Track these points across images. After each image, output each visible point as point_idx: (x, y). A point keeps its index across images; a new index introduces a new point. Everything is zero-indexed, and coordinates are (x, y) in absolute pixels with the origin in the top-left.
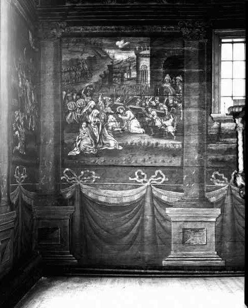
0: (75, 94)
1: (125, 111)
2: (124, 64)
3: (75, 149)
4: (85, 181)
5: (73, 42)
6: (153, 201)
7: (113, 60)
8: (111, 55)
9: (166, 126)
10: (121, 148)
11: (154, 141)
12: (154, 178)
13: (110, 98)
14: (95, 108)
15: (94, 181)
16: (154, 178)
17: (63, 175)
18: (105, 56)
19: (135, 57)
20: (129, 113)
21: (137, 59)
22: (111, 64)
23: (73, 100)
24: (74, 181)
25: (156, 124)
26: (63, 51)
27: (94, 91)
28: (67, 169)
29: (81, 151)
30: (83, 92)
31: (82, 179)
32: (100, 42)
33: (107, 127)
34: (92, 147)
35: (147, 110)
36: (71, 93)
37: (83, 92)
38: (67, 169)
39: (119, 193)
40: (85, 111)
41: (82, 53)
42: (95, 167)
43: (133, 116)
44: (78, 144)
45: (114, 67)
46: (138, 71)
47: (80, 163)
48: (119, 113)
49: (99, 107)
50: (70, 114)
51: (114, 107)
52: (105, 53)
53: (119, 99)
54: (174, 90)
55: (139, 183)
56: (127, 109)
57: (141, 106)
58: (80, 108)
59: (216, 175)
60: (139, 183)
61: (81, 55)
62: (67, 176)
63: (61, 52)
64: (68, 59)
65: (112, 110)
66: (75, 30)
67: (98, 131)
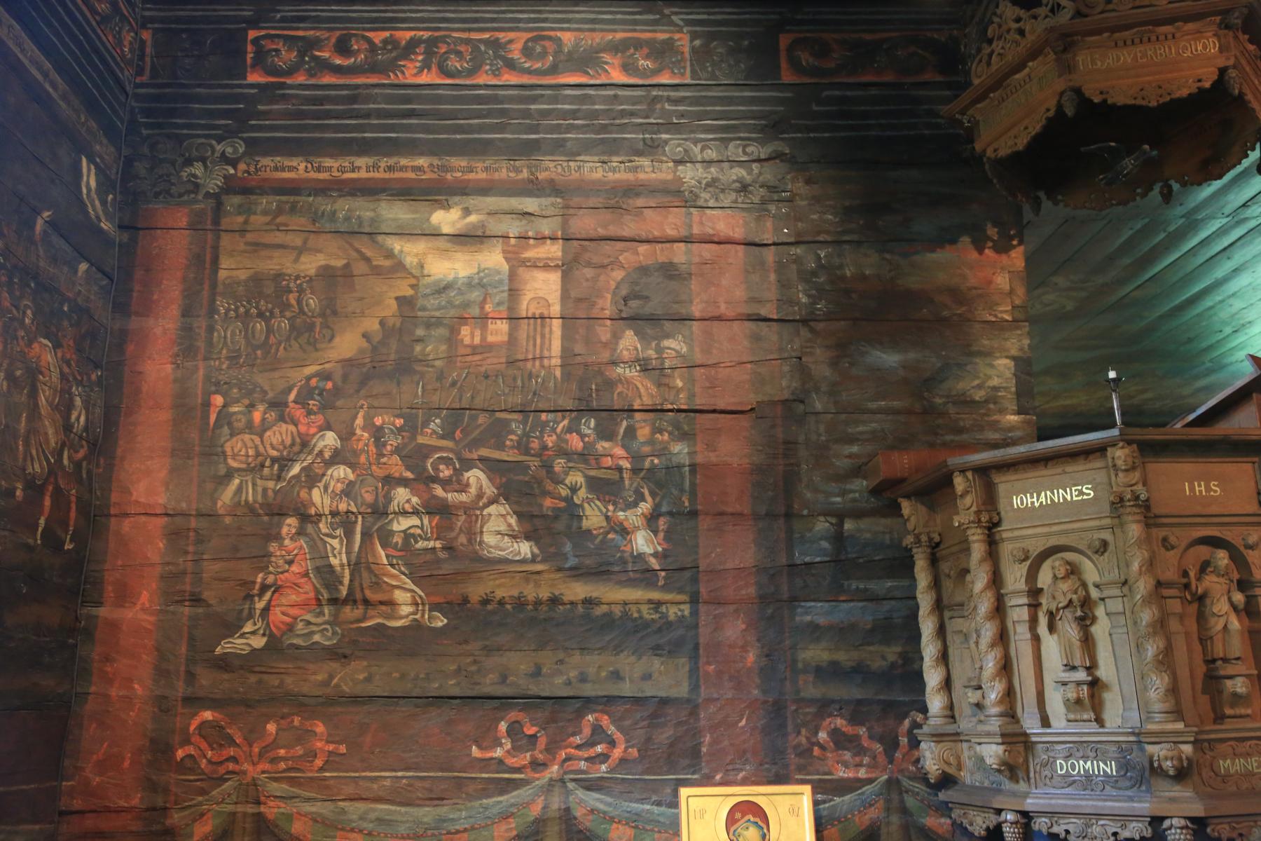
0: (261, 408)
1: (458, 473)
2: (461, 292)
3: (248, 628)
4: (283, 765)
5: (265, 213)
7: (416, 276)
8: (410, 261)
9: (624, 532)
10: (440, 622)
11: (578, 590)
12: (578, 747)
13: (399, 422)
14: (337, 458)
15: (319, 762)
16: (578, 747)
17: (187, 741)
18: (387, 263)
19: (506, 267)
20: (476, 477)
21: (512, 275)
22: (410, 292)
23: (250, 427)
24: (231, 766)
25: (586, 524)
26: (226, 241)
27: (337, 392)
28: (208, 715)
29: (271, 636)
30: (292, 397)
31: (271, 755)
32: (369, 214)
33: (386, 537)
34: (319, 620)
35: (548, 467)
36: (247, 402)
37: (292, 397)
38: (208, 715)
39: (427, 814)
40: (296, 470)
41: (300, 251)
42: (331, 703)
43: (490, 490)
44: (260, 605)
45: (420, 302)
46: (513, 319)
47: (255, 690)
48: (435, 479)
49: (356, 453)
50: (237, 481)
51: (415, 456)
52: (389, 254)
53: (435, 424)
54: (654, 390)
55: (518, 770)
56: (467, 465)
57: (527, 453)
58: (274, 460)
59: (835, 733)
60: (518, 770)
61: (296, 260)
62: (204, 745)
63: (216, 248)
64: (243, 275)
65: (408, 468)
66: (276, 169)
67: (348, 553)
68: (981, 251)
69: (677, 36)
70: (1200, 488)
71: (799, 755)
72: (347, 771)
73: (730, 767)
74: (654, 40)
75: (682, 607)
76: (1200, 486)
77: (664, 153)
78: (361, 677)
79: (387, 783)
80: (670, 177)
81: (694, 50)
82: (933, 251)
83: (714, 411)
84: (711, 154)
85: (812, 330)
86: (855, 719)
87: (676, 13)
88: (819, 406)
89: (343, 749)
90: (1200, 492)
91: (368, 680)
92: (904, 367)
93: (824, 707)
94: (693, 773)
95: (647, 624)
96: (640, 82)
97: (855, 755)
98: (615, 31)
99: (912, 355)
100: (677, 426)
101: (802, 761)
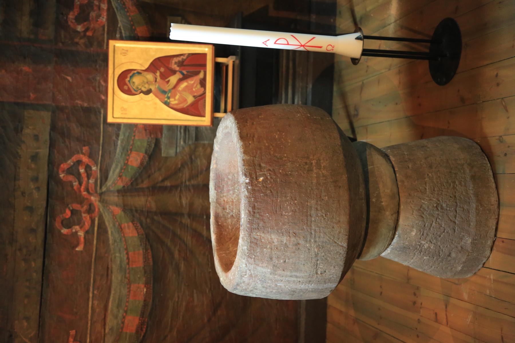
6: (142, 190)
12: (80, 184)
16: (80, 184)
39: (116, 277)
71: (91, 45)
72: (87, 328)
73: (97, 89)
78: (26, 324)
79: (96, 303)
86: (70, 6)
89: (73, 332)
91: (27, 319)
93: (61, 25)
94: (100, 113)
97: (93, 9)
101: (95, 44)
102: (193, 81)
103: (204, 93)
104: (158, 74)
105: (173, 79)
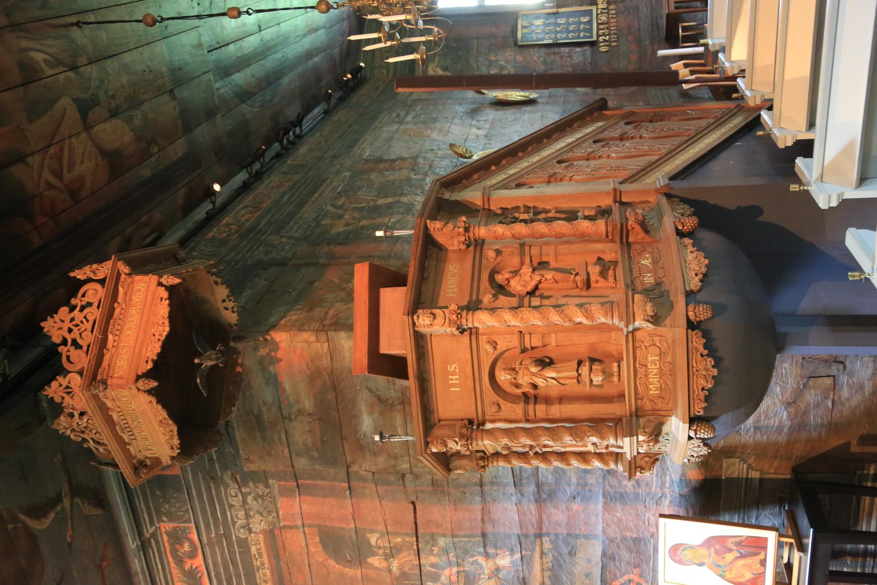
68: (281, 360)
69: (163, 530)
70: (454, 379)
74: (169, 542)
75: (544, 541)
76: (452, 379)
77: (247, 538)
80: (261, 536)
81: (171, 520)
82: (285, 390)
83: (416, 523)
84: (241, 514)
85: (353, 463)
87: (147, 530)
88: (406, 466)
90: (456, 379)
92: (372, 413)
95: (555, 559)
96: (200, 550)
98: (168, 563)
99: (363, 407)
100: (427, 543)
102: (754, 561)
103: (763, 574)
104: (712, 550)
105: (730, 557)
